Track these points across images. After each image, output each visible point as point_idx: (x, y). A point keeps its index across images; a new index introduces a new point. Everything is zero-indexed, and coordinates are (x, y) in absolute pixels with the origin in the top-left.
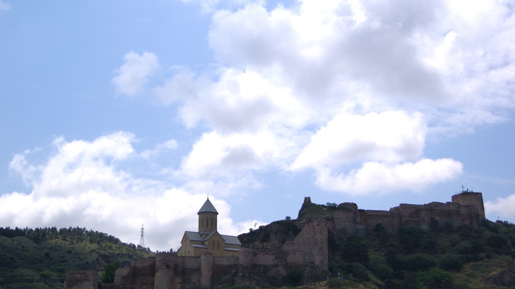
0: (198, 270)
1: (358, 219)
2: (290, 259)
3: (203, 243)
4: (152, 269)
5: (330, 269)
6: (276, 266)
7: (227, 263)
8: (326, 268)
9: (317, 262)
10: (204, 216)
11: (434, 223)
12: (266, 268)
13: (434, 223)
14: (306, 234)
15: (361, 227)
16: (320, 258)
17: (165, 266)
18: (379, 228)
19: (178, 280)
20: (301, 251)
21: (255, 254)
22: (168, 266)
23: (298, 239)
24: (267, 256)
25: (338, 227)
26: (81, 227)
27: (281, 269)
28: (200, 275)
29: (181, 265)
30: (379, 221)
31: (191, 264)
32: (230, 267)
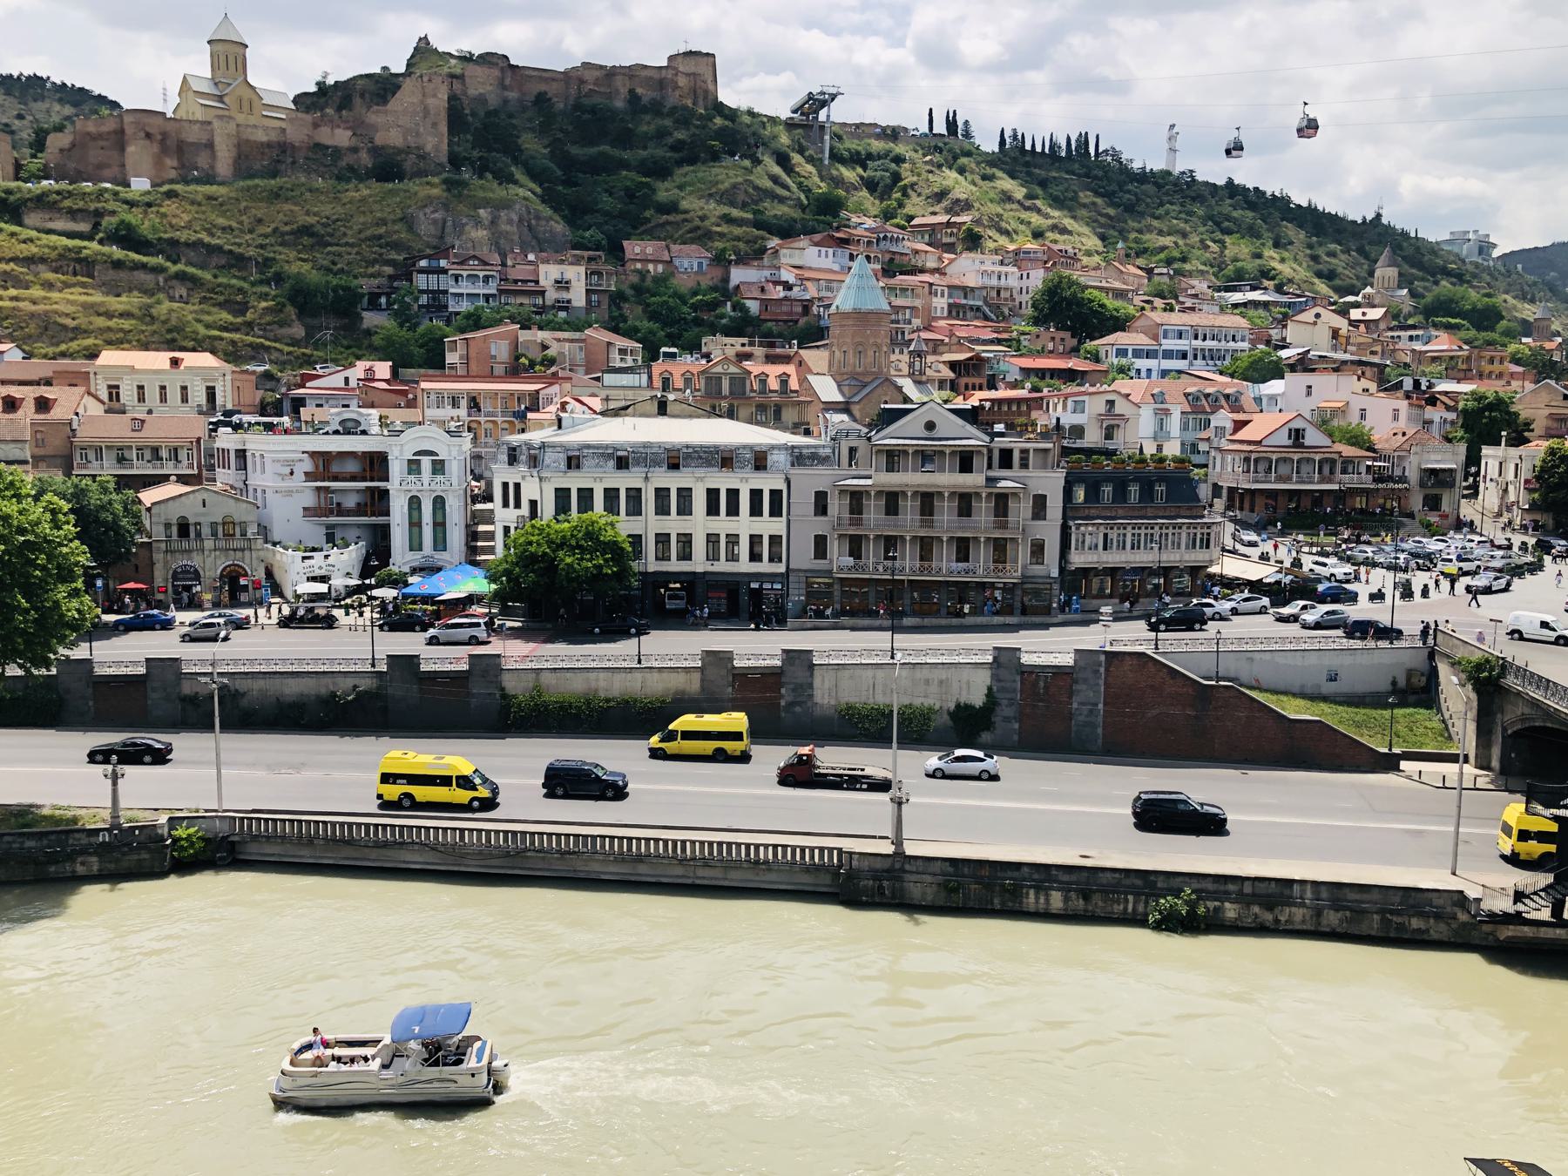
0: (210, 145)
1: (508, 82)
2: (379, 140)
3: (220, 98)
4: (119, 140)
5: (450, 161)
6: (355, 150)
7: (264, 139)
8: (444, 160)
9: (429, 148)
10: (219, 47)
11: (633, 97)
12: (337, 152)
13: (633, 97)
14: (407, 96)
15: (512, 95)
16: (436, 142)
17: (142, 134)
18: (541, 100)
19: (171, 162)
21: (316, 125)
22: (148, 136)
23: (394, 104)
24: (338, 131)
25: (472, 92)
26: (42, 74)
28: (213, 156)
30: (543, 87)
31: (193, 135)
32: (269, 145)
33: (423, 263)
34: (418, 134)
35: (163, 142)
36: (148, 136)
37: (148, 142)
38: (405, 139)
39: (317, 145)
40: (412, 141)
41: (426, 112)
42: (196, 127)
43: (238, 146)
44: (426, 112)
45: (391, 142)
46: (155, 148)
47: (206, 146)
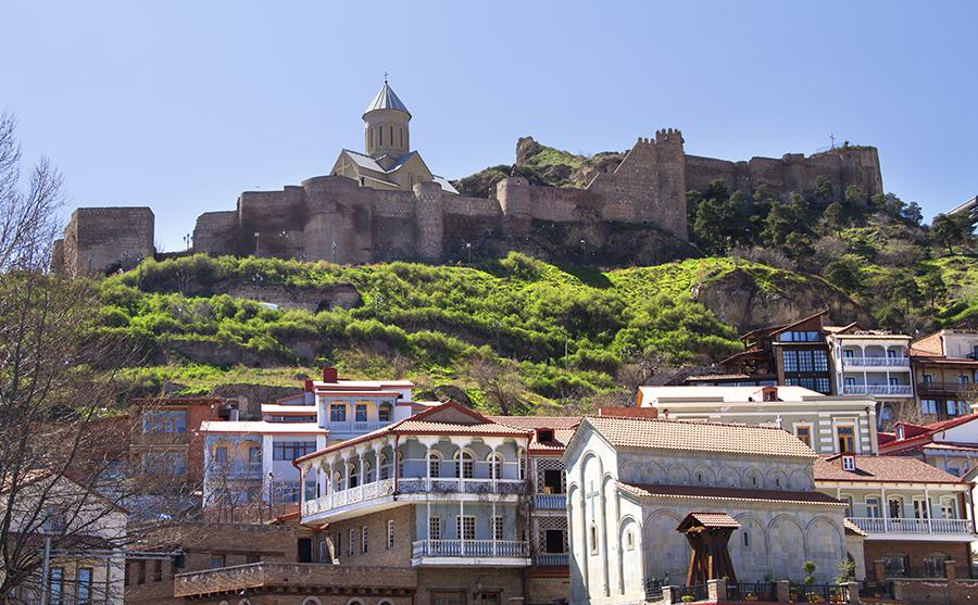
6: (580, 224)
20: (630, 197)
22: (340, 208)
27: (591, 233)
29: (368, 207)
33: (786, 337)
34: (652, 208)
35: (355, 217)
36: (340, 208)
37: (339, 216)
38: (638, 213)
39: (536, 222)
40: (644, 215)
41: (663, 180)
42: (393, 199)
43: (444, 221)
44: (663, 180)
45: (620, 216)
46: (348, 223)
47: (404, 221)
